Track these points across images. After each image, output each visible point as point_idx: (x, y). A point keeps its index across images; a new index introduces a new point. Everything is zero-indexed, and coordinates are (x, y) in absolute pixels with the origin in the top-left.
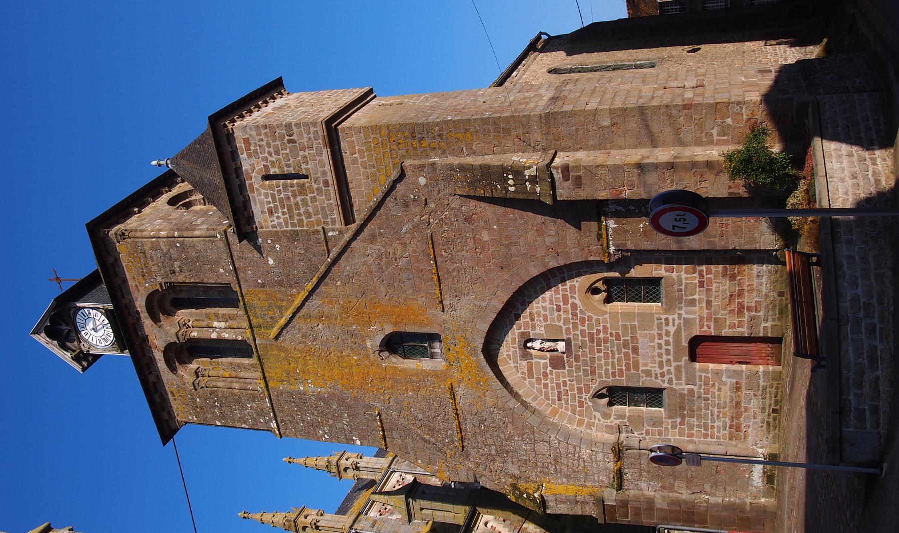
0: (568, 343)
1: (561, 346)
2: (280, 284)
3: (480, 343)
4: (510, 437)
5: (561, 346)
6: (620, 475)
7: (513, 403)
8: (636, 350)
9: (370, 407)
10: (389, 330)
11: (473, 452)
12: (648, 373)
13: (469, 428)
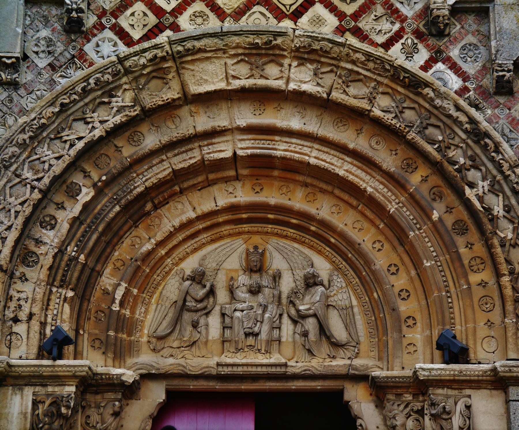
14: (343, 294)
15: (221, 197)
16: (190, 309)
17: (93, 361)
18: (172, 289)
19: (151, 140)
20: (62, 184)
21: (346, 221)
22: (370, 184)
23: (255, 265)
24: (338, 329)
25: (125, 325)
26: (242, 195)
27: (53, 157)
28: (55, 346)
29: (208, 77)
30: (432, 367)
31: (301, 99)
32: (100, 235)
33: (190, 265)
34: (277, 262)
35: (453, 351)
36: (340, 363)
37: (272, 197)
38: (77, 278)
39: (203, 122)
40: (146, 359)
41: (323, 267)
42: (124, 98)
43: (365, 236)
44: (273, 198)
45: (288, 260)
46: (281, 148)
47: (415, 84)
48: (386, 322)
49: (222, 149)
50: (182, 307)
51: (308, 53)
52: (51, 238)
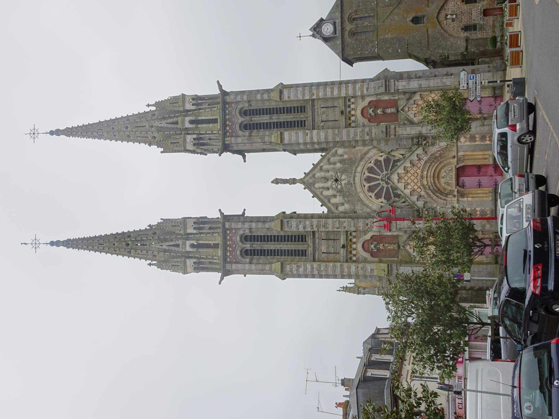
0: (456, 14)
1: (454, 16)
2: (388, 6)
3: (436, 16)
4: (440, 42)
5: (454, 16)
6: (467, 47)
7: (442, 31)
8: (471, 14)
9: (405, 39)
10: (414, 15)
11: (431, 49)
12: (474, 20)
13: (430, 40)
14: (446, 168)
15: (436, 181)
16: (448, 184)
17: (456, 193)
18: (446, 186)
19: (432, 188)
20: (437, 196)
21: (439, 168)
22: (436, 166)
23: (443, 178)
24: (450, 169)
25: (450, 190)
26: (436, 179)
27: (435, 197)
28: (454, 196)
29: (425, 183)
30: (456, 159)
31: (427, 173)
32: (442, 193)
33: (443, 184)
34: (443, 175)
35: (454, 157)
36: (454, 169)
37: (436, 176)
38: (447, 195)
39: (430, 183)
40: (454, 188)
41: (443, 170)
42: (428, 191)
43: (441, 166)
44: (437, 176)
45: (443, 174)
46: (432, 175)
47: (426, 161)
48: (450, 163)
49: (432, 181)
50: (448, 185)
51: (422, 172)
52: (443, 197)
